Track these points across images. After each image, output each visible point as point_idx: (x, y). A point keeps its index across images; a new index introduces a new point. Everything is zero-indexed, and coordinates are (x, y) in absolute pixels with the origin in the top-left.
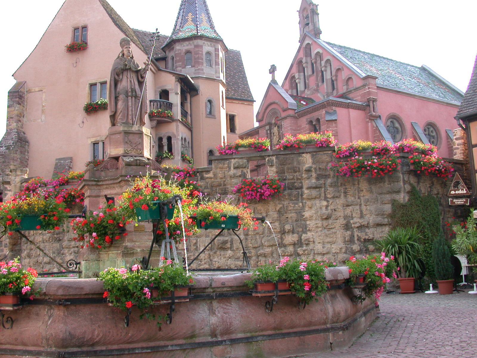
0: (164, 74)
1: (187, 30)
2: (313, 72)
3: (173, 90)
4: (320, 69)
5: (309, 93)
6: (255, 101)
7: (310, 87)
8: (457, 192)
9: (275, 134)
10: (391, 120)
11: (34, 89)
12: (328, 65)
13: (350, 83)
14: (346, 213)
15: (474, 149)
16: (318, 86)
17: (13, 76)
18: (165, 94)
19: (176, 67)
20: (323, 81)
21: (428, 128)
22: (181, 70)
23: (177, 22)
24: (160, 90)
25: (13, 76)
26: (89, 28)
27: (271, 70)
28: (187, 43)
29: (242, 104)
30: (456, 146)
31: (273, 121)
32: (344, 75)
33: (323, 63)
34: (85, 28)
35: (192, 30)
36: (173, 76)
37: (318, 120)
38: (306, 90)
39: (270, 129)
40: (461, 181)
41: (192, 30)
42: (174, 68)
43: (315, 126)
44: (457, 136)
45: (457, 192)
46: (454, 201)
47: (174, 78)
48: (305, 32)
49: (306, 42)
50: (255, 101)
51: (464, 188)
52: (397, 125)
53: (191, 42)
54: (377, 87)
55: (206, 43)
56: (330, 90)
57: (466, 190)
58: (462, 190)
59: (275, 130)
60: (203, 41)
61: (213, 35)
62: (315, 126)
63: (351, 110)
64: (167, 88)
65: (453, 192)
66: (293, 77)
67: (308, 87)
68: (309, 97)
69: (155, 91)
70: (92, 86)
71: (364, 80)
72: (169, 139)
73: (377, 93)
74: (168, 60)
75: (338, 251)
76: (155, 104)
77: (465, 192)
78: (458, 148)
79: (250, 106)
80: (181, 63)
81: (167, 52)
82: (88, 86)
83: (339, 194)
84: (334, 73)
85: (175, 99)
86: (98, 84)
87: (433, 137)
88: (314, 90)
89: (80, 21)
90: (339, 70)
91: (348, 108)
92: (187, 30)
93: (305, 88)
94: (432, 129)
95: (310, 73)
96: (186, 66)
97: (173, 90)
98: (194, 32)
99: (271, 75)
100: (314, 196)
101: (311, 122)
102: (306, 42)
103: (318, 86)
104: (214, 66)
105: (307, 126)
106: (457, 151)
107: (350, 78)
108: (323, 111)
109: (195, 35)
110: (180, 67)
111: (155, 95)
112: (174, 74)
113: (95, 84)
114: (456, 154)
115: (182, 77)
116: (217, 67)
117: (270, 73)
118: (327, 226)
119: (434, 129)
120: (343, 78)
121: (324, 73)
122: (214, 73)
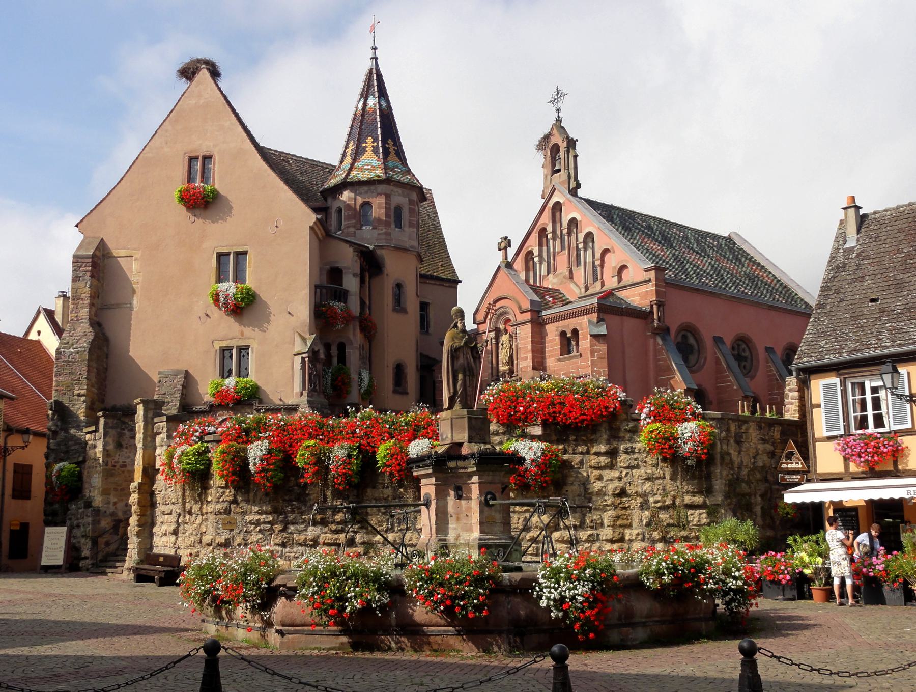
0: (335, 243)
1: (365, 167)
2: (563, 248)
3: (349, 269)
4: (575, 245)
5: (555, 280)
6: (461, 282)
7: (558, 272)
8: (790, 466)
9: (504, 346)
10: (683, 333)
11: (117, 251)
12: (589, 240)
13: (625, 274)
14: (645, 488)
15: (814, 410)
16: (571, 272)
17: (77, 226)
18: (335, 274)
19: (348, 227)
20: (578, 264)
21: (739, 345)
22: (355, 232)
23: (346, 148)
24: (328, 267)
25: (77, 226)
26: (217, 158)
27: (503, 245)
28: (366, 188)
29: (440, 285)
30: (790, 400)
31: (502, 327)
32: (612, 261)
33: (581, 237)
34: (207, 158)
35: (374, 168)
36: (350, 246)
37: (575, 332)
38: (551, 276)
39: (497, 338)
40: (796, 451)
41: (374, 168)
42: (343, 227)
43: (569, 339)
44: (791, 387)
45: (790, 466)
46: (786, 477)
47: (351, 249)
48: (553, 183)
49: (555, 199)
50: (461, 282)
51: (800, 460)
52: (692, 341)
53: (373, 188)
54: (666, 283)
55: (396, 190)
56: (590, 280)
57: (802, 464)
58: (798, 463)
59: (505, 338)
60: (392, 188)
61: (406, 179)
62: (569, 339)
63: (625, 318)
64: (340, 265)
65: (784, 466)
66: (530, 253)
67: (555, 271)
68: (556, 287)
69: (321, 270)
70: (221, 257)
71: (646, 271)
72: (342, 347)
73: (665, 292)
74: (331, 213)
75: (633, 538)
76: (324, 291)
77: (800, 466)
78: (792, 404)
79: (452, 290)
80: (354, 221)
81: (329, 200)
82: (215, 256)
83: (636, 462)
84: (598, 255)
85: (351, 283)
86: (231, 256)
87: (745, 359)
88: (564, 277)
89: (202, 147)
90: (606, 251)
91: (622, 315)
92: (365, 167)
93: (549, 273)
94: (744, 346)
95: (558, 248)
96: (362, 226)
97: (349, 269)
98: (380, 172)
99: (501, 253)
100: (602, 464)
101: (563, 334)
102: (555, 199)
103: (571, 272)
104: (406, 229)
105: (558, 338)
106: (790, 406)
107: (624, 267)
108: (584, 319)
109: (379, 177)
110: (354, 227)
111: (321, 275)
112: (351, 244)
113: (228, 254)
114: (788, 411)
115: (364, 249)
116: (411, 229)
117: (500, 250)
118: (619, 504)
119: (747, 346)
120: (614, 265)
121: (582, 252)
122: (406, 239)
